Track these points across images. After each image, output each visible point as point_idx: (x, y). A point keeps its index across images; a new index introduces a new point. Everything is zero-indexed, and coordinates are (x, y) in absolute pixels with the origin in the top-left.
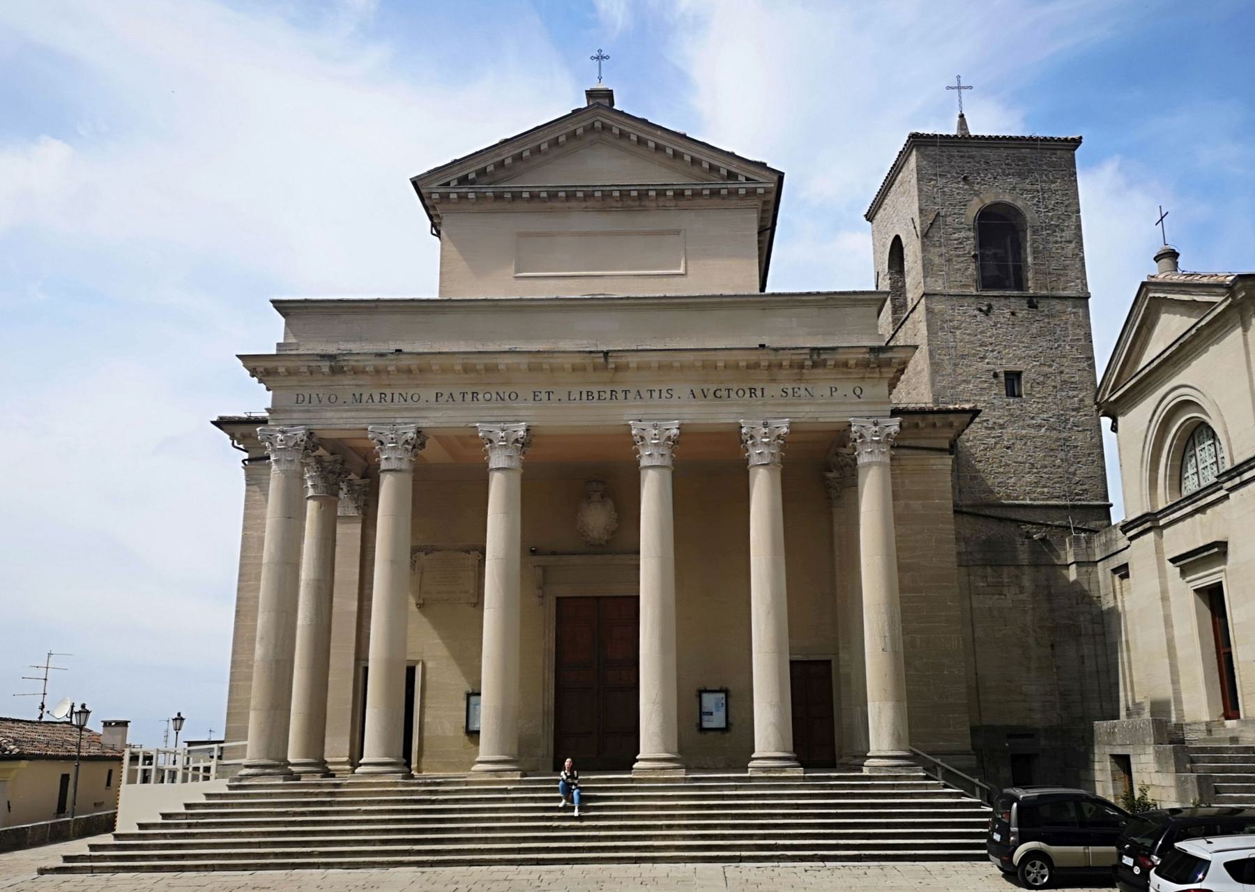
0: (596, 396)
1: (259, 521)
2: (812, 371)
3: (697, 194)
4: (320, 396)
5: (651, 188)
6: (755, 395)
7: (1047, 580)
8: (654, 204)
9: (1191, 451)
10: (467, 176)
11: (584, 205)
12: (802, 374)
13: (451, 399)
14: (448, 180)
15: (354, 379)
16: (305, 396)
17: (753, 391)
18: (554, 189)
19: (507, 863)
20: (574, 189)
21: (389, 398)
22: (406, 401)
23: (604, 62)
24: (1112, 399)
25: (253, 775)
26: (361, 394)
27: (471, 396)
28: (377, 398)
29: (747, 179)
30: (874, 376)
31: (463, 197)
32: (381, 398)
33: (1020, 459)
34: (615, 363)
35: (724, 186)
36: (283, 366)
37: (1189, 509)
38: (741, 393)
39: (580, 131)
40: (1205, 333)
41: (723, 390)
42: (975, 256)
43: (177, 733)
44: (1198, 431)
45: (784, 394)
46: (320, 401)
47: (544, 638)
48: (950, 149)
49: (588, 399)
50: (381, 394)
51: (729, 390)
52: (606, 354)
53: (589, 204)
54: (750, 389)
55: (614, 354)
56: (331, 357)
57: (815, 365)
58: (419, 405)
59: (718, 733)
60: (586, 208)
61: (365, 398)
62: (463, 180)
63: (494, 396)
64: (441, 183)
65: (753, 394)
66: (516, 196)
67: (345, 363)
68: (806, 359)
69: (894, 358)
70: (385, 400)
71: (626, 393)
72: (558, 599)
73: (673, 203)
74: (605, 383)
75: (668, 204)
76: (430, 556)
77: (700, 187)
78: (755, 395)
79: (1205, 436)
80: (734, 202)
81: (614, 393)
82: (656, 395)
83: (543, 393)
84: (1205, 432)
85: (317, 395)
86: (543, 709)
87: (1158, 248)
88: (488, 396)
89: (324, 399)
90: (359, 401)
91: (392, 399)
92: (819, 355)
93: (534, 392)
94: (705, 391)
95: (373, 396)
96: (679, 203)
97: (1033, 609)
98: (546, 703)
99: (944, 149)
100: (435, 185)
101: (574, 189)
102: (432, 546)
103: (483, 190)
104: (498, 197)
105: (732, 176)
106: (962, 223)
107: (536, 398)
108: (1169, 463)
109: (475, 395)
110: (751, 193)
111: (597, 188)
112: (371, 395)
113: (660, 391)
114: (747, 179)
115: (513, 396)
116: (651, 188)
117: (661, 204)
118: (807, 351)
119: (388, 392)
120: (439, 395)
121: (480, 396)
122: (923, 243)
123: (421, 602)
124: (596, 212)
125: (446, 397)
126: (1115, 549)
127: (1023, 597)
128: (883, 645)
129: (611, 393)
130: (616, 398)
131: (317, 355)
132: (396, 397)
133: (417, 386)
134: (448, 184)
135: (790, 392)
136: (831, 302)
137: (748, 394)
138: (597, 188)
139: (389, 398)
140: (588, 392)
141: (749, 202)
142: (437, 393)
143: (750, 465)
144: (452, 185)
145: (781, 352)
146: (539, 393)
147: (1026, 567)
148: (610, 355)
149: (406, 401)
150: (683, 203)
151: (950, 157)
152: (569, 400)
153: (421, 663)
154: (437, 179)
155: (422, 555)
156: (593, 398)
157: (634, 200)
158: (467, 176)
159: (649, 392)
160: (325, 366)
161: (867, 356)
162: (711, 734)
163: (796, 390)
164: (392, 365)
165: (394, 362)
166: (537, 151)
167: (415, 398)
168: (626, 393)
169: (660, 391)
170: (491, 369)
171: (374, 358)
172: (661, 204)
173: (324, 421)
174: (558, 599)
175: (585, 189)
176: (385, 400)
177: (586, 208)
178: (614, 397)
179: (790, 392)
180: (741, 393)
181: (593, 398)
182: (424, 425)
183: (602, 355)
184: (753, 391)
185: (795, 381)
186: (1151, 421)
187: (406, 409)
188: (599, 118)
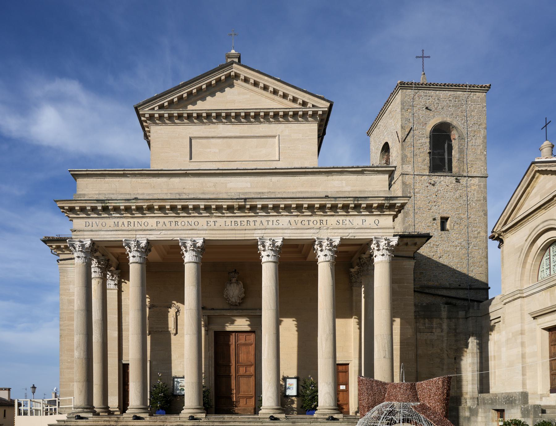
0: (239, 224)
4: (97, 223)
5: (261, 110)
6: (323, 223)
13: (164, 225)
16: (90, 223)
17: (321, 221)
21: (132, 224)
22: (141, 226)
26: (118, 222)
27: (175, 223)
28: (126, 224)
32: (128, 224)
38: (315, 222)
41: (306, 221)
42: (429, 153)
43: (33, 394)
45: (338, 223)
46: (97, 226)
47: (209, 351)
49: (235, 225)
50: (128, 222)
51: (309, 221)
58: (149, 227)
61: (120, 224)
62: (161, 107)
63: (186, 223)
65: (321, 223)
66: (190, 116)
70: (130, 225)
71: (255, 222)
72: (215, 332)
78: (323, 223)
81: (248, 222)
82: (270, 223)
88: (183, 223)
89: (99, 224)
90: (117, 226)
91: (134, 225)
93: (207, 221)
94: (296, 221)
95: (124, 223)
100: (147, 109)
104: (180, 117)
106: (423, 134)
107: (208, 225)
109: (177, 223)
111: (233, 111)
113: (273, 221)
115: (196, 223)
120: (158, 223)
121: (179, 223)
122: (402, 145)
125: (162, 223)
128: (385, 355)
129: (247, 222)
130: (250, 225)
132: (136, 223)
134: (153, 109)
135: (341, 222)
137: (319, 224)
138: (233, 111)
139: (132, 224)
140: (235, 221)
142: (157, 222)
143: (319, 261)
146: (209, 222)
149: (141, 226)
152: (225, 225)
154: (148, 106)
156: (238, 224)
159: (267, 221)
167: (146, 224)
168: (255, 222)
169: (273, 221)
174: (215, 332)
176: (130, 225)
178: (248, 224)
179: (341, 222)
180: (315, 222)
181: (238, 224)
182: (151, 239)
184: (321, 221)
187: (141, 230)
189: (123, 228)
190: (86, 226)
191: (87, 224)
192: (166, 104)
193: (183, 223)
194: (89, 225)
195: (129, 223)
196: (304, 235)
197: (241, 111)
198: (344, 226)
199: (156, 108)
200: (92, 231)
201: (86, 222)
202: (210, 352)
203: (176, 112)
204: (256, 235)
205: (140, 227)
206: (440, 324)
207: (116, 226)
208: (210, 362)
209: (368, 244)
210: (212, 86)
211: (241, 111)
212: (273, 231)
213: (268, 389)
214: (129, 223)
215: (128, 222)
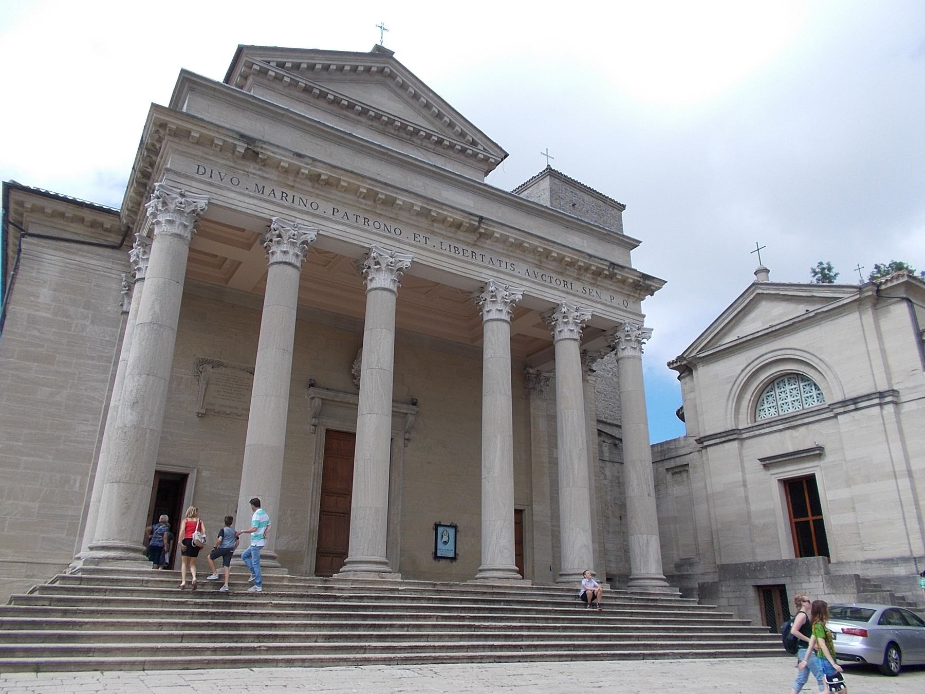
1: (32, 298)
2: (603, 280)
3: (452, 147)
7: (618, 472)
8: (419, 142)
9: (768, 392)
10: (285, 63)
11: (370, 123)
12: (596, 280)
13: (345, 217)
14: (269, 59)
15: (259, 170)
18: (354, 102)
19: (468, 661)
20: (369, 108)
23: (385, 32)
24: (702, 355)
25: (121, 559)
26: (264, 187)
29: (484, 149)
30: (634, 295)
31: (278, 79)
33: (599, 390)
34: (486, 229)
35: (471, 148)
36: (198, 132)
37: (781, 427)
39: (374, 69)
40: (820, 316)
44: (778, 381)
45: (584, 292)
48: (567, 185)
50: (283, 192)
52: (481, 218)
53: (374, 124)
54: (564, 281)
55: (486, 222)
56: (249, 140)
57: (611, 276)
59: (448, 561)
60: (371, 126)
61: (267, 191)
62: (281, 65)
63: (383, 226)
64: (263, 59)
66: (323, 95)
67: (262, 151)
68: (606, 270)
69: (653, 286)
73: (433, 147)
74: (468, 244)
75: (429, 146)
76: (216, 370)
77: (456, 142)
79: (787, 383)
80: (472, 161)
82: (503, 265)
83: (421, 237)
84: (786, 381)
85: (220, 173)
86: (310, 529)
87: (757, 267)
92: (613, 268)
96: (436, 148)
97: (611, 491)
98: (312, 522)
99: (563, 183)
100: (258, 59)
101: (369, 108)
102: (219, 362)
103: (298, 79)
104: (307, 90)
105: (474, 143)
108: (752, 399)
110: (486, 159)
112: (273, 190)
114: (484, 149)
116: (422, 129)
117: (424, 144)
118: (608, 264)
119: (290, 193)
120: (336, 210)
123: (204, 411)
124: (377, 133)
126: (674, 454)
127: (606, 482)
131: (237, 133)
133: (318, 196)
135: (587, 291)
136: (607, 237)
141: (481, 165)
144: (271, 64)
145: (593, 258)
147: (607, 463)
148: (483, 221)
150: (439, 149)
151: (566, 189)
153: (196, 471)
155: (209, 367)
157: (407, 134)
158: (285, 63)
160: (241, 148)
161: (639, 279)
162: (443, 562)
163: (591, 291)
164: (306, 168)
165: (309, 167)
166: (341, 69)
167: (315, 206)
170: (390, 202)
171: (292, 156)
172: (424, 144)
173: (226, 199)
175: (377, 111)
177: (371, 126)
183: (477, 219)
185: (591, 284)
186: (743, 371)
188: (389, 66)
189: (272, 198)
190: (198, 173)
191: (202, 170)
192: (288, 65)
193: (377, 225)
194: (204, 174)
195: (285, 195)
196: (547, 295)
197: (396, 119)
198: (590, 297)
199: (274, 64)
200: (210, 184)
201: (199, 166)
202: (317, 464)
203: (305, 82)
204: (486, 275)
205: (302, 207)
206: (603, 468)
207: (259, 192)
208: (315, 484)
209: (604, 331)
210: (344, 72)
211: (396, 119)
212: (507, 277)
213: (501, 532)
214: (285, 195)
215: (283, 192)
